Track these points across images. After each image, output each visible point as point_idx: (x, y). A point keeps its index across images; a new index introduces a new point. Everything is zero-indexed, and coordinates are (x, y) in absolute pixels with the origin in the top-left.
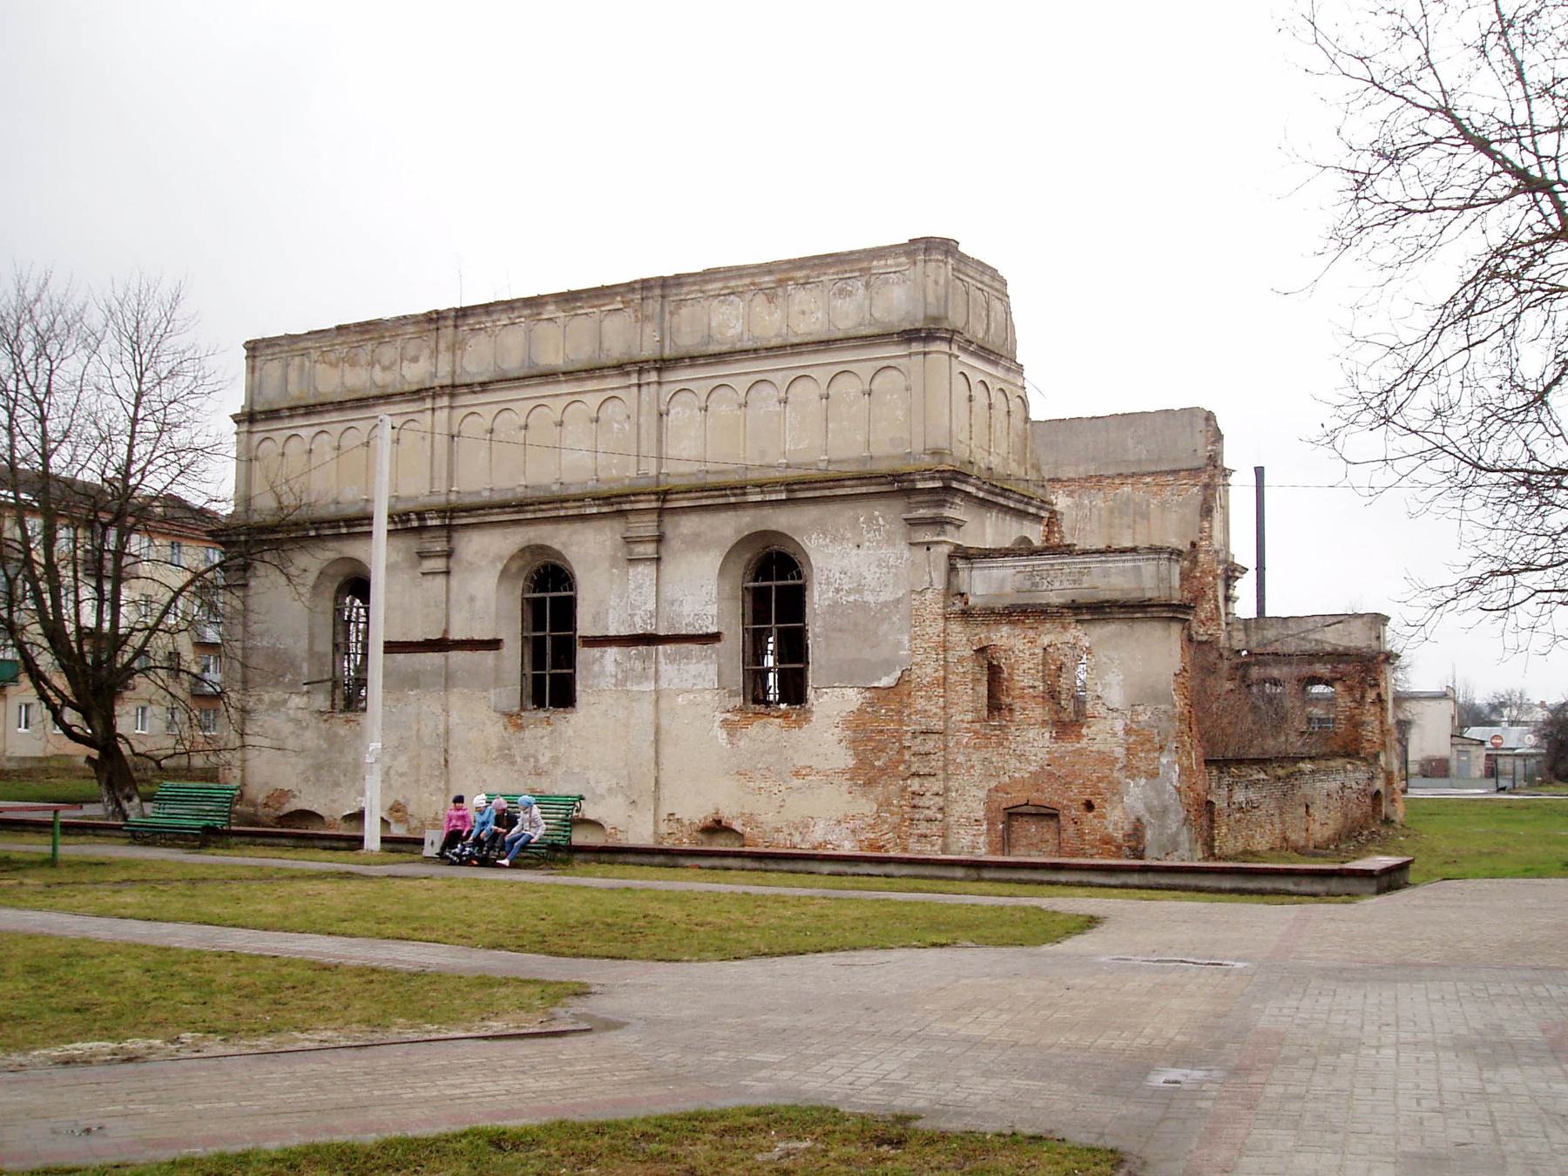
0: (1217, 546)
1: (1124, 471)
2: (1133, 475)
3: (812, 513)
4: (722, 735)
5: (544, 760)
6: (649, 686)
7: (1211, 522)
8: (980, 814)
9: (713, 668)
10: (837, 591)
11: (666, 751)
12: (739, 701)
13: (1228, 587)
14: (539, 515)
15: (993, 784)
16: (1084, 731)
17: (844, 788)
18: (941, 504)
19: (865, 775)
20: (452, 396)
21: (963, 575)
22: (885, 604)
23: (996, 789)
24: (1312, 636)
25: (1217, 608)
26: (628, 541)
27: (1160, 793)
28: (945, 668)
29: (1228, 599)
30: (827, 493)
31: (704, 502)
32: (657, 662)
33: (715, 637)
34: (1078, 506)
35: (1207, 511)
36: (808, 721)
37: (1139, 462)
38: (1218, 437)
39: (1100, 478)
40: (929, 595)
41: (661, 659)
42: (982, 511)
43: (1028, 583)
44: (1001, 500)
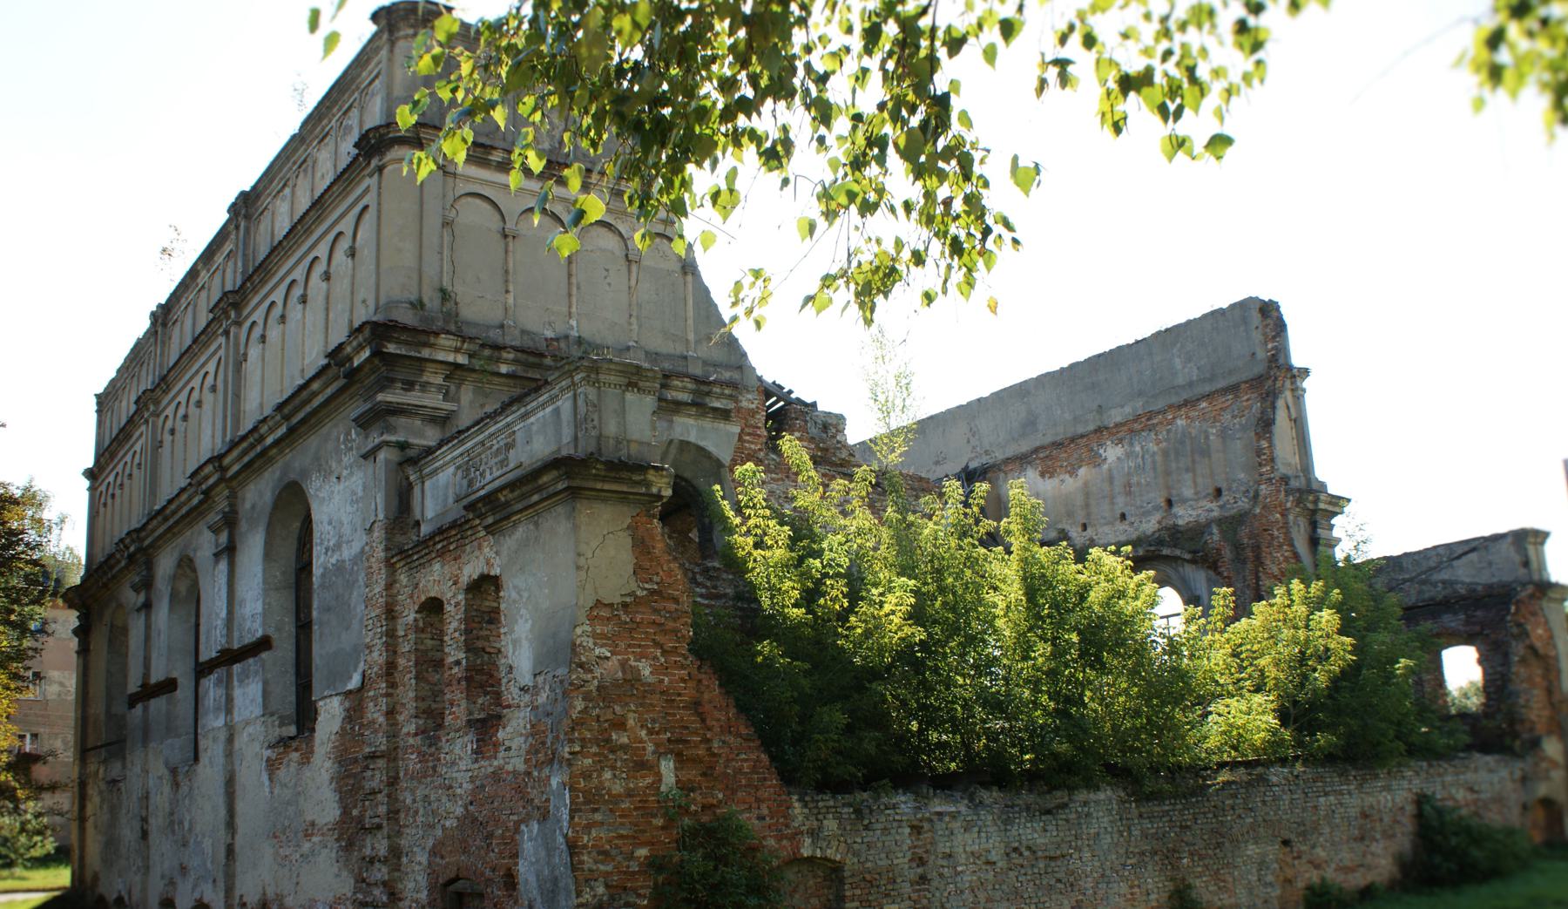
0: (1282, 470)
1: (1174, 400)
2: (1186, 403)
3: (313, 442)
4: (265, 777)
5: (186, 826)
6: (220, 722)
7: (1270, 440)
8: (423, 896)
9: (260, 686)
10: (327, 550)
11: (240, 806)
12: (292, 730)
13: (1314, 525)
14: (176, 517)
15: (430, 843)
16: (501, 735)
17: (333, 855)
18: (385, 383)
19: (351, 831)
20: (157, 402)
21: (417, 490)
22: (356, 556)
23: (434, 852)
24: (1436, 577)
25: (1296, 556)
26: (215, 530)
27: (550, 851)
28: (391, 647)
29: (1314, 542)
30: (308, 409)
31: (246, 459)
32: (229, 687)
33: (263, 644)
34: (1128, 455)
35: (1265, 425)
36: (312, 752)
37: (1191, 384)
38: (1280, 327)
39: (1151, 415)
40: (376, 534)
41: (236, 683)
43: (465, 482)
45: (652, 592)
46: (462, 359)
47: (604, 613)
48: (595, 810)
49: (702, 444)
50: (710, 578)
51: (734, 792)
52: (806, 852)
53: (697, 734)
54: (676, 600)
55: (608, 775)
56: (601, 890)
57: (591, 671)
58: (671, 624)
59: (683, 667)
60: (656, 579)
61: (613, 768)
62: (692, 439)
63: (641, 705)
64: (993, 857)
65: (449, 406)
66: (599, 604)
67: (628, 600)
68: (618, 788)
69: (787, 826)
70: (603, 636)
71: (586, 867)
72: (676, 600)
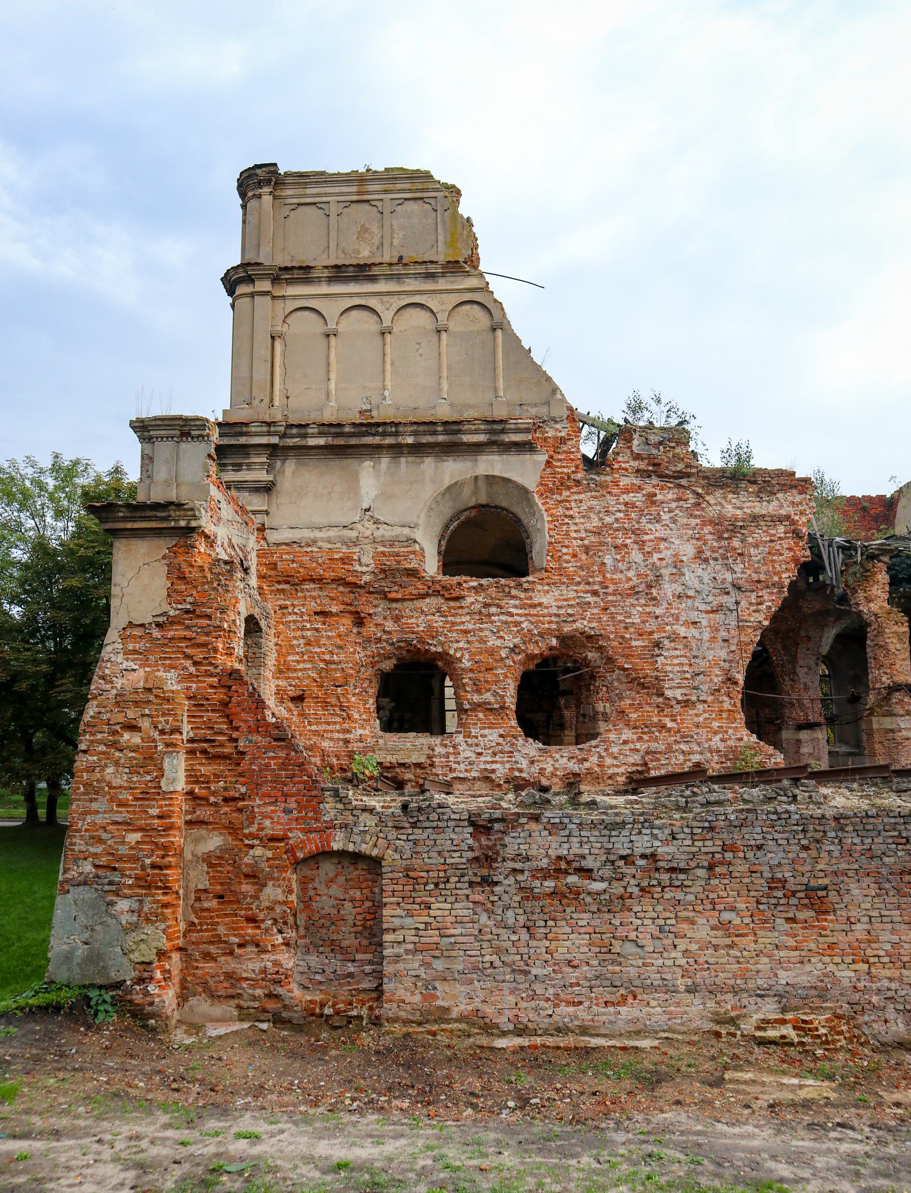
42: (351, 463)
44: (369, 440)
45: (187, 612)
46: (275, 440)
47: (137, 632)
48: (91, 800)
49: (506, 475)
50: (526, 590)
51: (258, 785)
52: (336, 846)
53: (221, 733)
54: (209, 617)
55: (110, 770)
56: (87, 867)
57: (112, 682)
58: (204, 639)
59: (211, 675)
60: (189, 599)
61: (117, 763)
62: (497, 473)
63: (156, 710)
64: (589, 863)
65: (270, 478)
66: (131, 625)
67: (160, 619)
68: (117, 782)
69: (317, 820)
70: (135, 652)
71: (76, 848)
72: (209, 617)
